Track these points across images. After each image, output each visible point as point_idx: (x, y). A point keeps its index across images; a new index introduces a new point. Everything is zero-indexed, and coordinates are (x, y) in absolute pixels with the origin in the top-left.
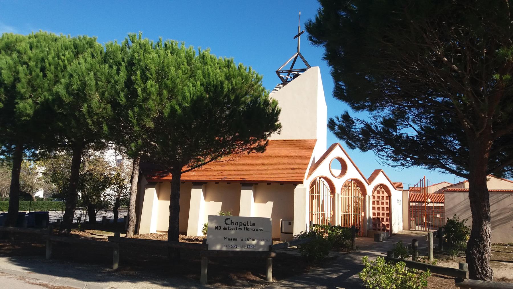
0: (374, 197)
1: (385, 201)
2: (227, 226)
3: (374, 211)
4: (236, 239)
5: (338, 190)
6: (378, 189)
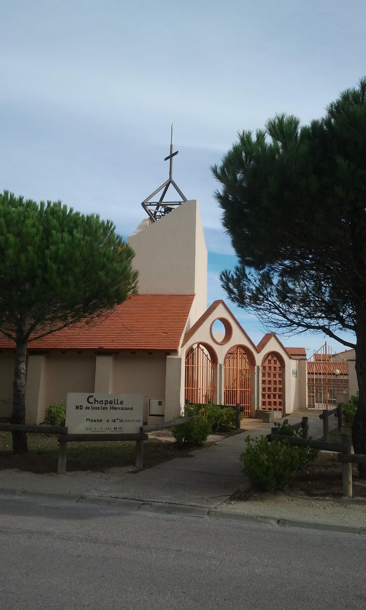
0: (264, 368)
1: (278, 379)
2: (90, 405)
3: (264, 386)
4: (101, 421)
5: (221, 360)
6: (270, 357)
